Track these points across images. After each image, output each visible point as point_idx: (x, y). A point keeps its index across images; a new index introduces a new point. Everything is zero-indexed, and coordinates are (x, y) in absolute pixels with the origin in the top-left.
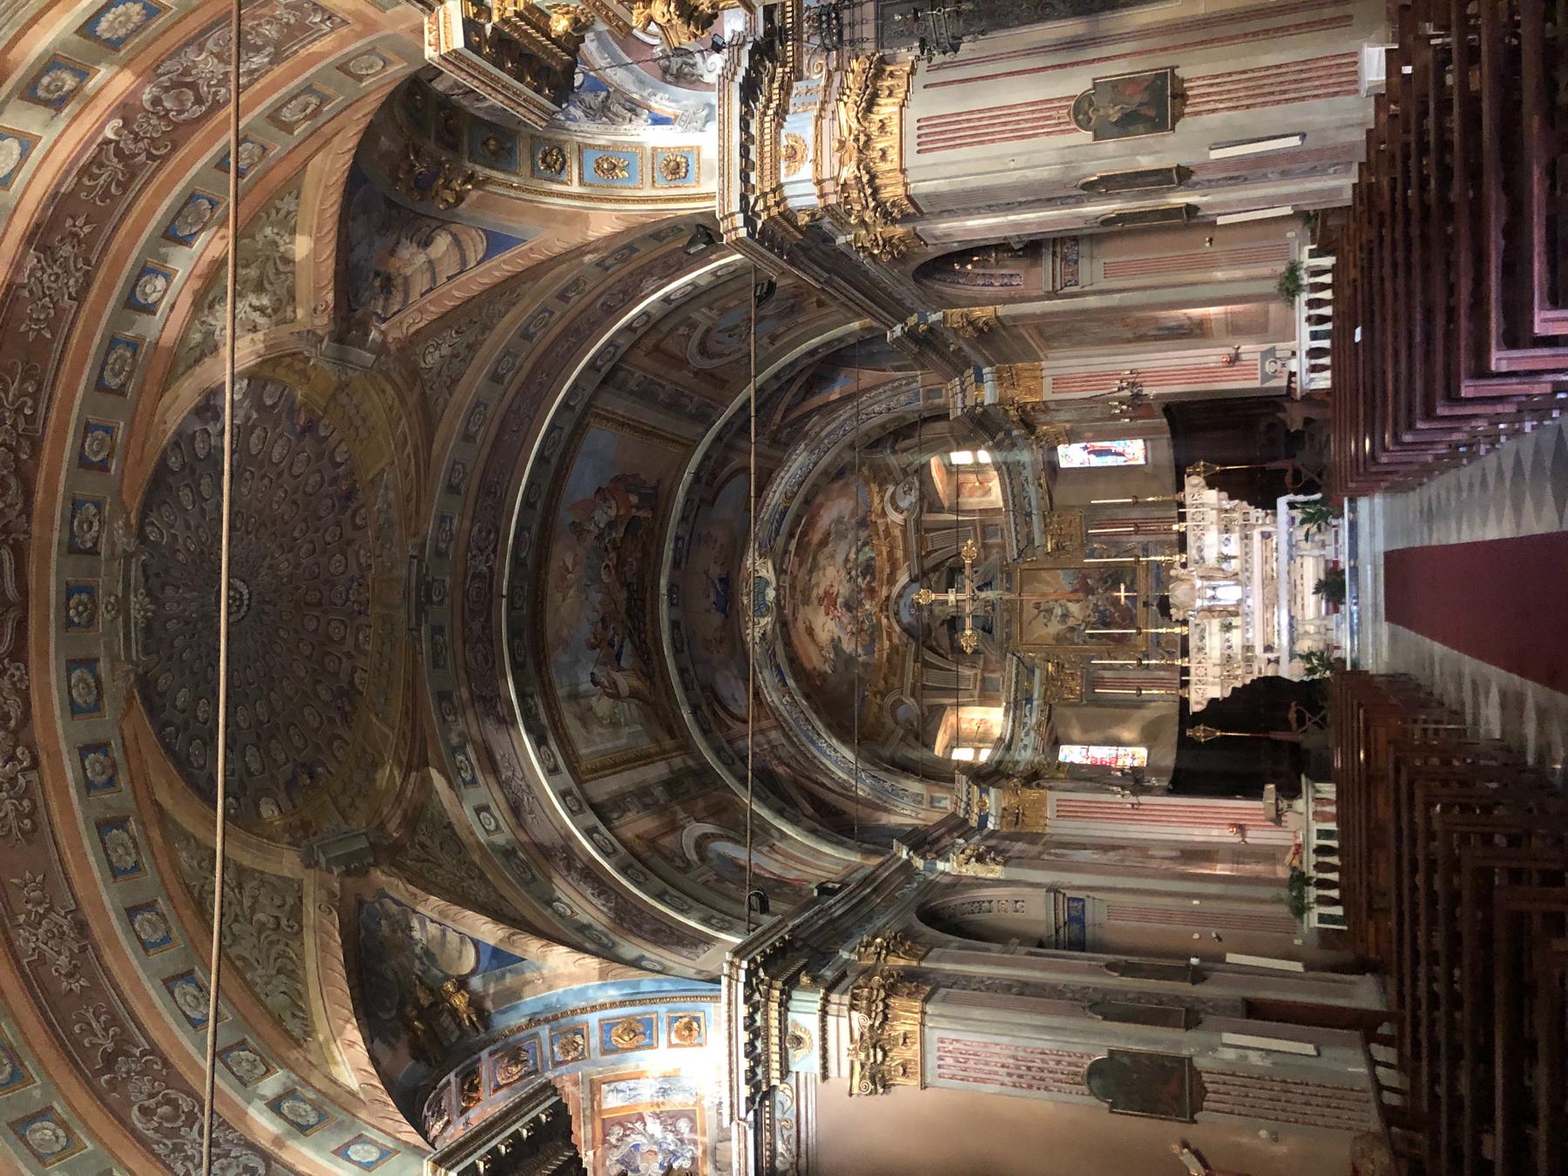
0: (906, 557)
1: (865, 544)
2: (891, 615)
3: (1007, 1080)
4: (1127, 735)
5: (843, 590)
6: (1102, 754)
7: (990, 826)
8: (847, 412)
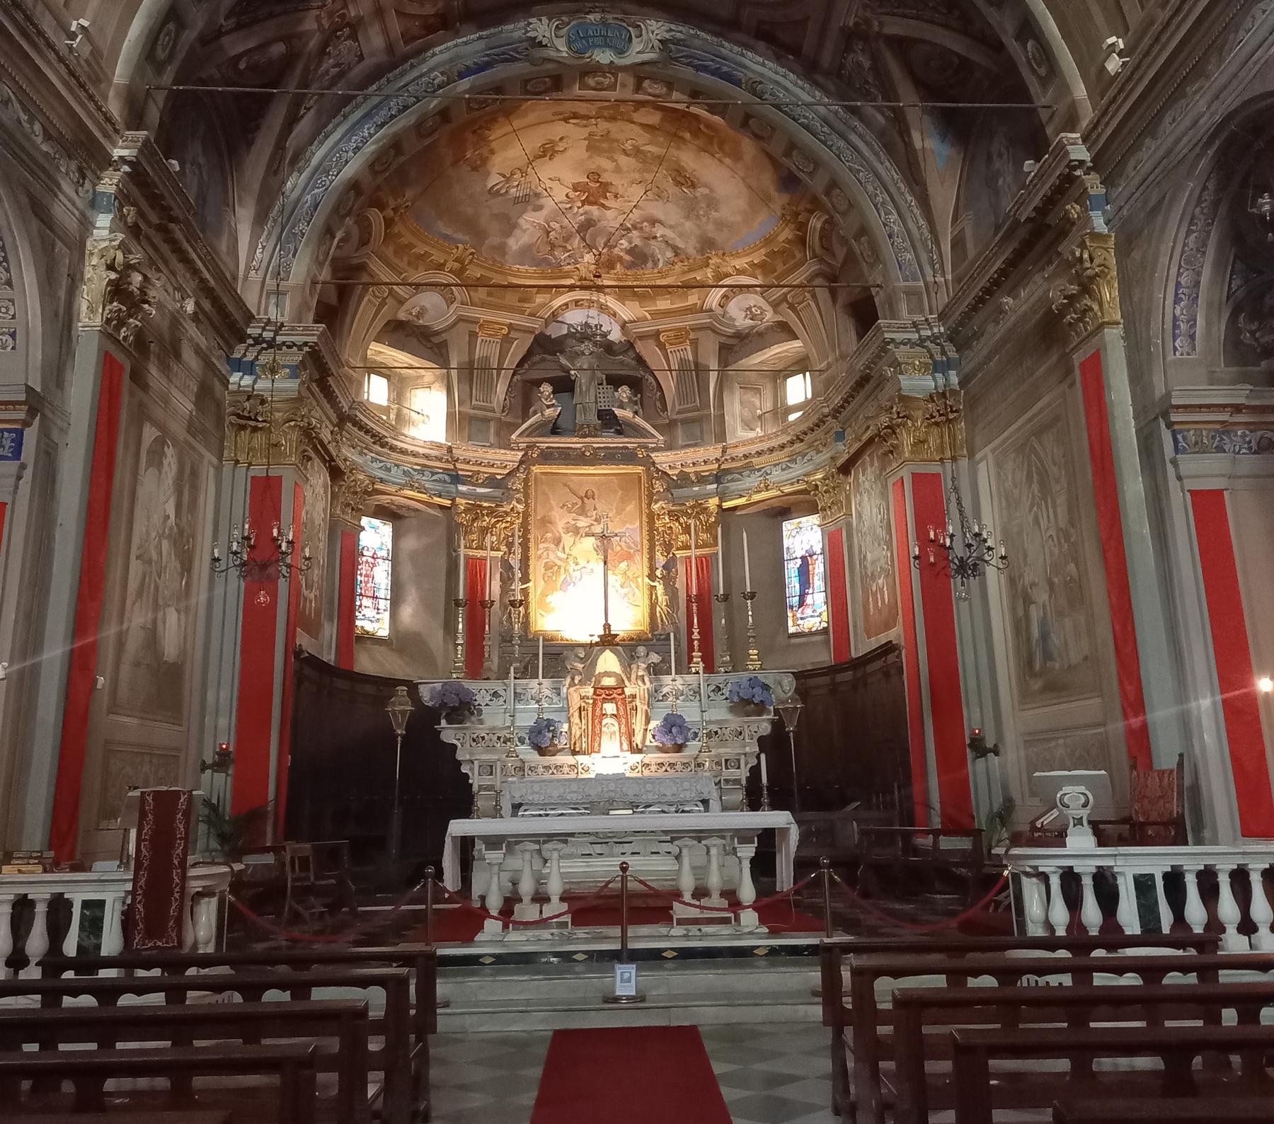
0: (656, 315)
4: (407, 612)
5: (610, 218)
6: (380, 576)
7: (235, 378)
8: (889, 171)
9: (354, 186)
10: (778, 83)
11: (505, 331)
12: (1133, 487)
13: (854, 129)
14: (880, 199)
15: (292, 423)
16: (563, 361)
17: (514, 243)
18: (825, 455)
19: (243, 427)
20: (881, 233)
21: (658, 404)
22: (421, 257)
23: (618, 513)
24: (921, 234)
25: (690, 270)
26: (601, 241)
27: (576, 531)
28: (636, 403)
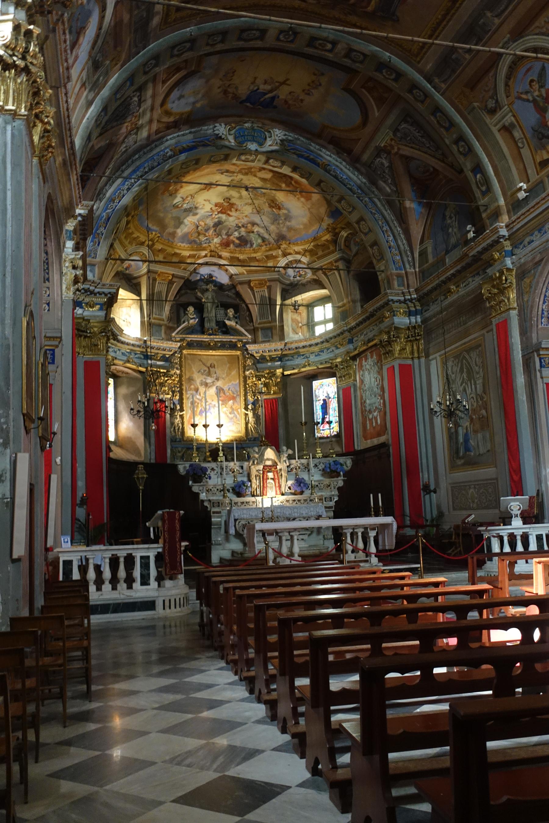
9: (126, 208)
10: (337, 166)
11: (170, 278)
12: (520, 380)
13: (373, 192)
14: (385, 229)
15: (104, 334)
16: (199, 294)
17: (180, 232)
18: (342, 350)
19: (81, 336)
20: (385, 245)
21: (247, 318)
22: (135, 239)
23: (227, 375)
24: (405, 248)
25: (270, 250)
26: (224, 232)
27: (206, 385)
28: (236, 318)
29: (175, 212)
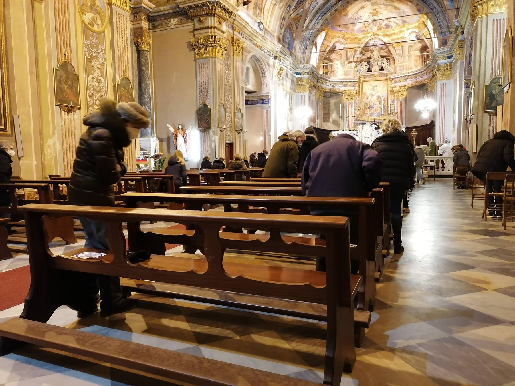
1: (397, 24)
2: (373, 37)
3: (200, 82)
29: (351, 21)
